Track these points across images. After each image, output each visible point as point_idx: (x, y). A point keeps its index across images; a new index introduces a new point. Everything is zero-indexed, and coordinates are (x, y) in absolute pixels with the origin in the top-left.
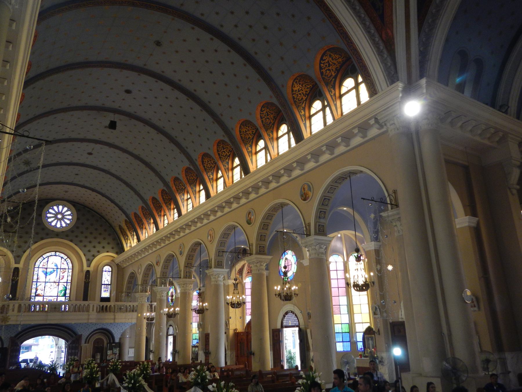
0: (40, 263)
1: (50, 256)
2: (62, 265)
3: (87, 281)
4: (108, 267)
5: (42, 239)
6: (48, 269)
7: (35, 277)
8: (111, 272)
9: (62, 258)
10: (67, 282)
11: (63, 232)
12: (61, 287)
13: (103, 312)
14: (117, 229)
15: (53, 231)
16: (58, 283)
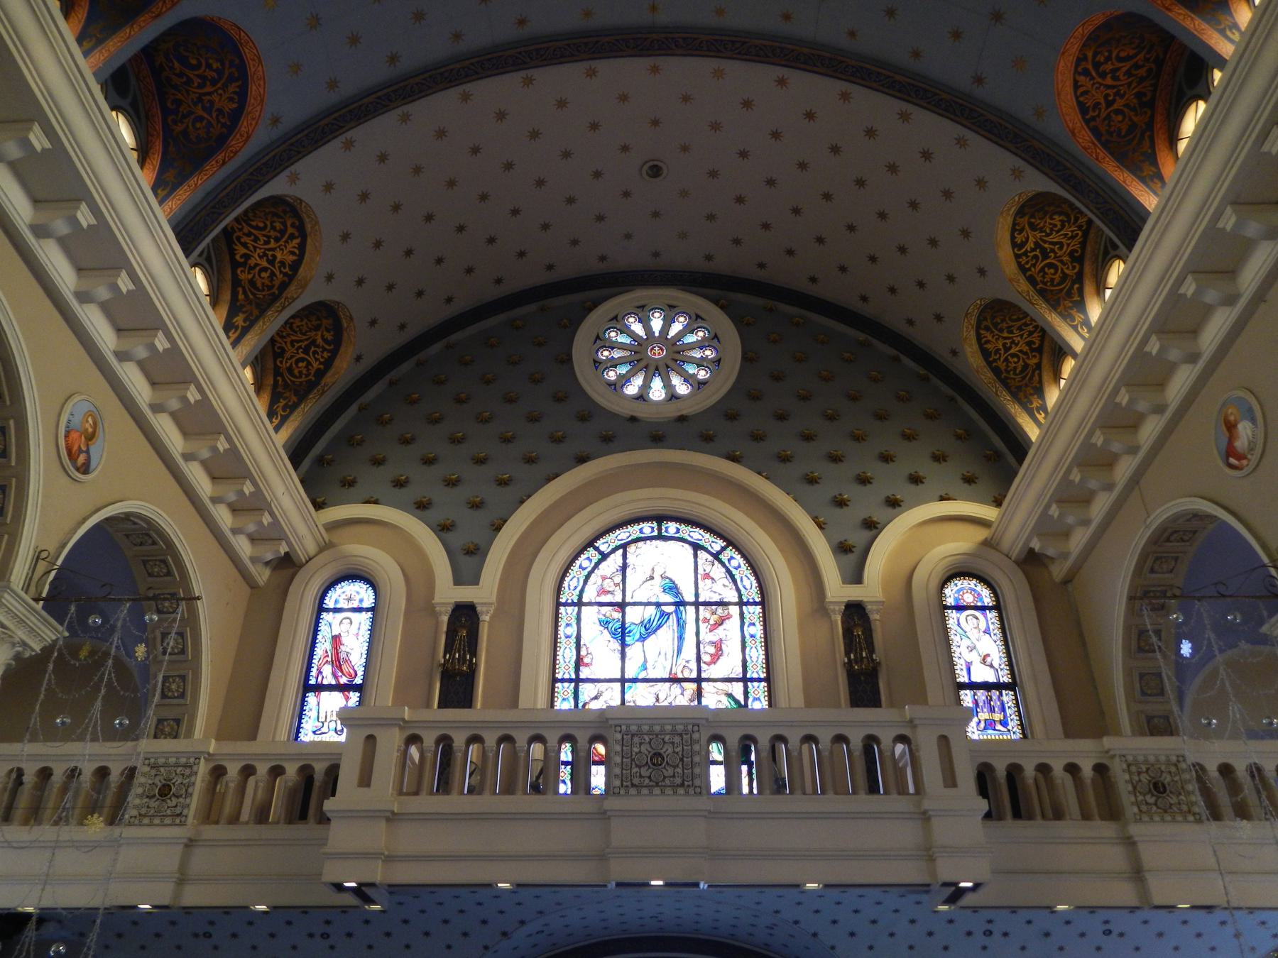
2: (704, 585)
3: (859, 660)
5: (582, 460)
6: (628, 609)
7: (567, 654)
8: (992, 615)
9: (696, 547)
10: (745, 680)
11: (682, 419)
13: (1031, 817)
15: (633, 419)
16: (694, 686)
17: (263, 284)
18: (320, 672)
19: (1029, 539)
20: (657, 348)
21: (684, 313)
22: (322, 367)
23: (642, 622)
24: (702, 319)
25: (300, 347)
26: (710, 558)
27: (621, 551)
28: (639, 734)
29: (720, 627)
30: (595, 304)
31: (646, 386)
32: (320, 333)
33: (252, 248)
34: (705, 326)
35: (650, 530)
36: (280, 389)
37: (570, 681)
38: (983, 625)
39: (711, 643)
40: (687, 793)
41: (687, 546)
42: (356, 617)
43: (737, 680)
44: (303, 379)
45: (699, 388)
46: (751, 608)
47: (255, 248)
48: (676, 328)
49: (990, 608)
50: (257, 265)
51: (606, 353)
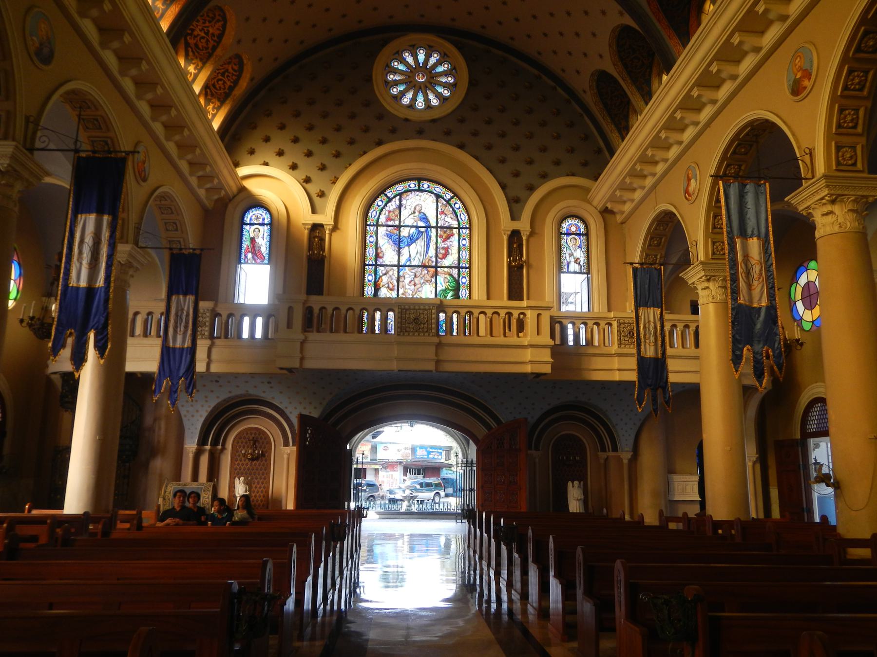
0: (382, 212)
1: (405, 192)
4: (576, 221)
5: (380, 143)
6: (402, 229)
7: (371, 252)
9: (438, 196)
10: (459, 267)
11: (434, 121)
12: (443, 282)
14: (590, 99)
15: (407, 120)
17: (203, 47)
18: (246, 257)
19: (606, 202)
20: (421, 75)
21: (437, 51)
22: (232, 84)
23: (409, 236)
24: (448, 56)
25: (219, 73)
26: (444, 202)
27: (398, 197)
28: (409, 309)
29: (449, 240)
30: (385, 43)
31: (414, 99)
32: (230, 66)
33: (195, 25)
34: (449, 61)
35: (414, 185)
36: (209, 97)
37: (372, 265)
38: (578, 244)
39: (443, 248)
40: (429, 335)
41: (433, 195)
42: (260, 227)
43: (455, 267)
44: (222, 91)
45: (443, 102)
46: (464, 231)
47: (197, 25)
48: (433, 60)
49: (583, 235)
50: (198, 35)
51: (392, 76)
